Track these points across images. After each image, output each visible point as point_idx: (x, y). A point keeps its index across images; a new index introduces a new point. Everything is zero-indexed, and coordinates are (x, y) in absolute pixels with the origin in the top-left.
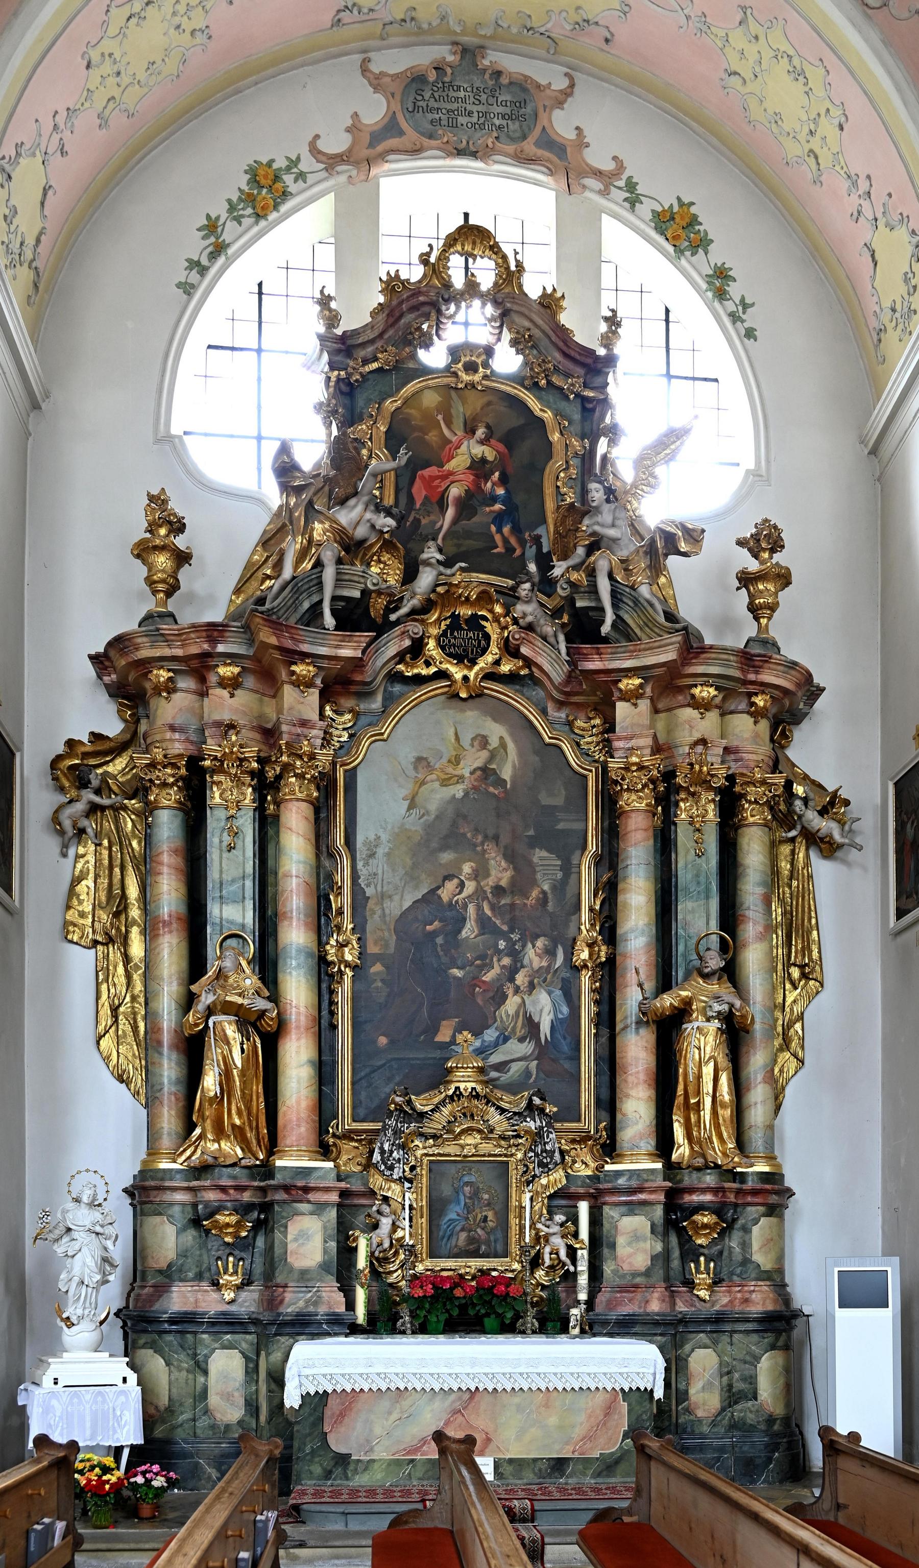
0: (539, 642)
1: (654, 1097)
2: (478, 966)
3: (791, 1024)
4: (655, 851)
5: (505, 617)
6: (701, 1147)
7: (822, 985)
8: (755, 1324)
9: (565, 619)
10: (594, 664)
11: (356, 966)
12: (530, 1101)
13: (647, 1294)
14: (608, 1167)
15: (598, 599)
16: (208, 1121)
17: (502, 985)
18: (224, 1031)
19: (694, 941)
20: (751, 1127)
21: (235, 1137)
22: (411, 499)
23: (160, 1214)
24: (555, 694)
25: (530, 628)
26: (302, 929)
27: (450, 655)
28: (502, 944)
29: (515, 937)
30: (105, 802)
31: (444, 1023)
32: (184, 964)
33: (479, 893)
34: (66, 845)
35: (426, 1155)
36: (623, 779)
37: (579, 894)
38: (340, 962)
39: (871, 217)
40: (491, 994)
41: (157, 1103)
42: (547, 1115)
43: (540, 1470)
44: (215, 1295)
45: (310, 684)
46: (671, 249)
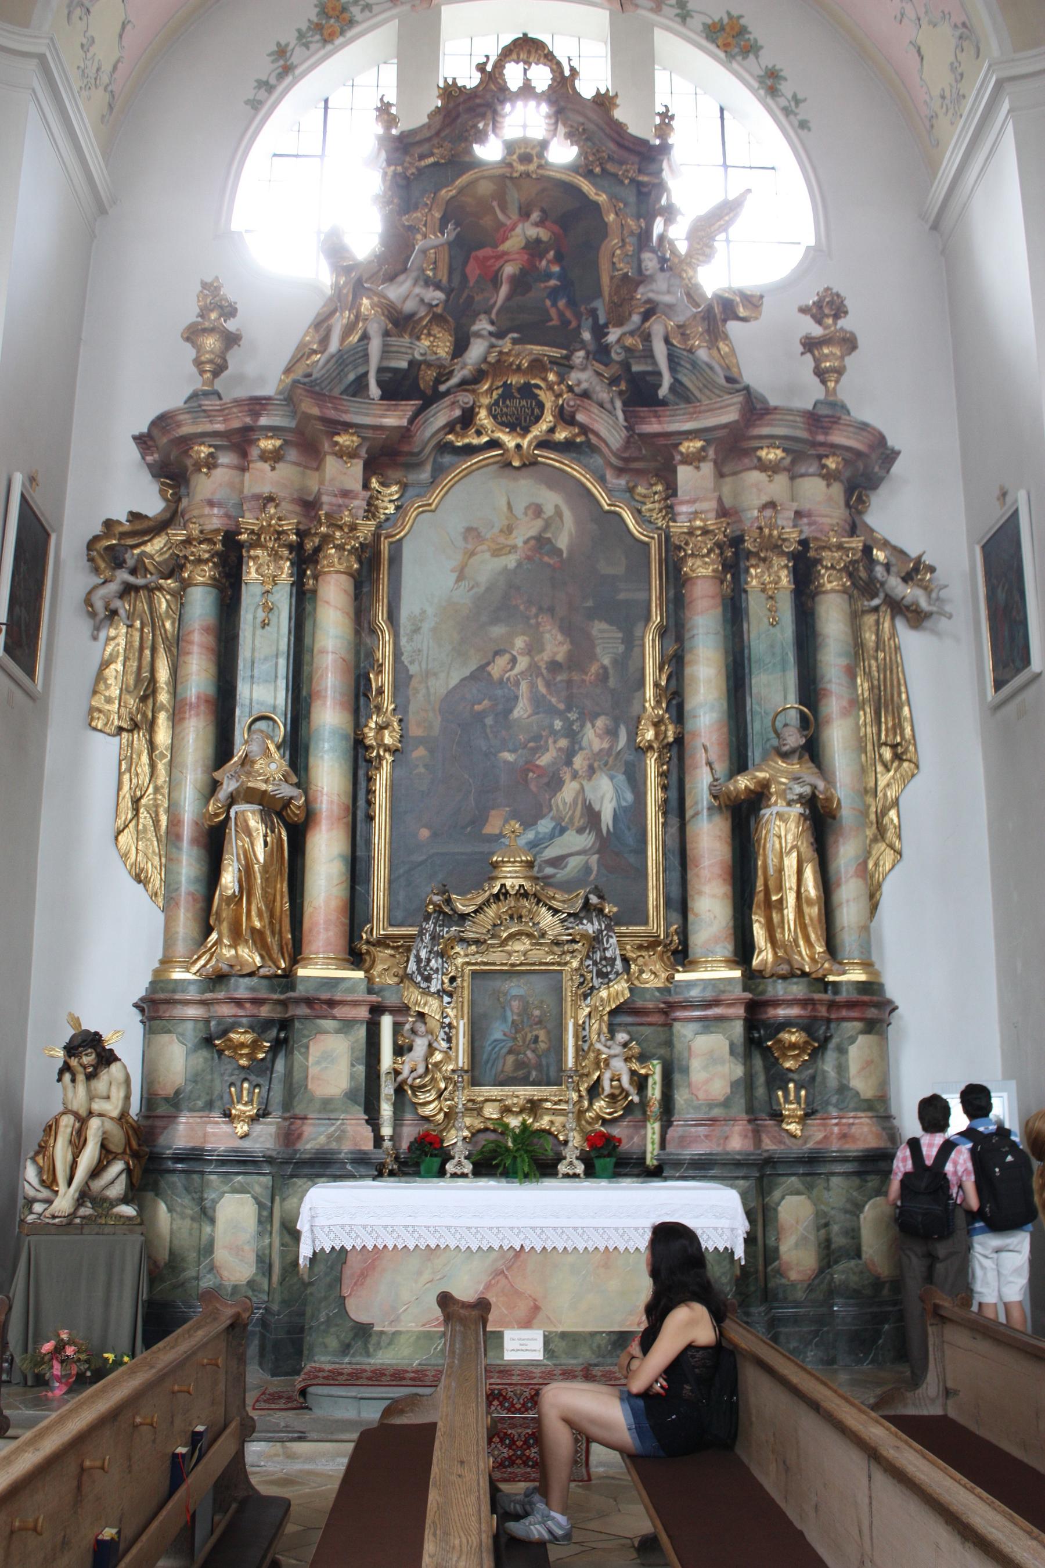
0: (595, 409)
2: (532, 749)
3: (884, 812)
4: (725, 621)
5: (559, 384)
7: (917, 767)
8: (856, 1164)
9: (623, 387)
10: (653, 427)
11: (397, 750)
12: (587, 900)
13: (726, 1128)
14: (679, 977)
15: (655, 363)
17: (559, 770)
19: (771, 717)
21: (254, 943)
22: (464, 278)
23: (169, 1032)
24: (614, 460)
25: (586, 395)
27: (503, 424)
28: (558, 724)
29: (573, 716)
30: (140, 581)
31: (493, 812)
32: (209, 751)
33: (533, 669)
34: (97, 628)
35: (468, 964)
36: (687, 544)
37: (643, 669)
38: (379, 746)
39: (914, 17)
40: (545, 780)
42: (606, 916)
43: (599, 1347)
44: (225, 1128)
45: (353, 455)
46: (722, 55)
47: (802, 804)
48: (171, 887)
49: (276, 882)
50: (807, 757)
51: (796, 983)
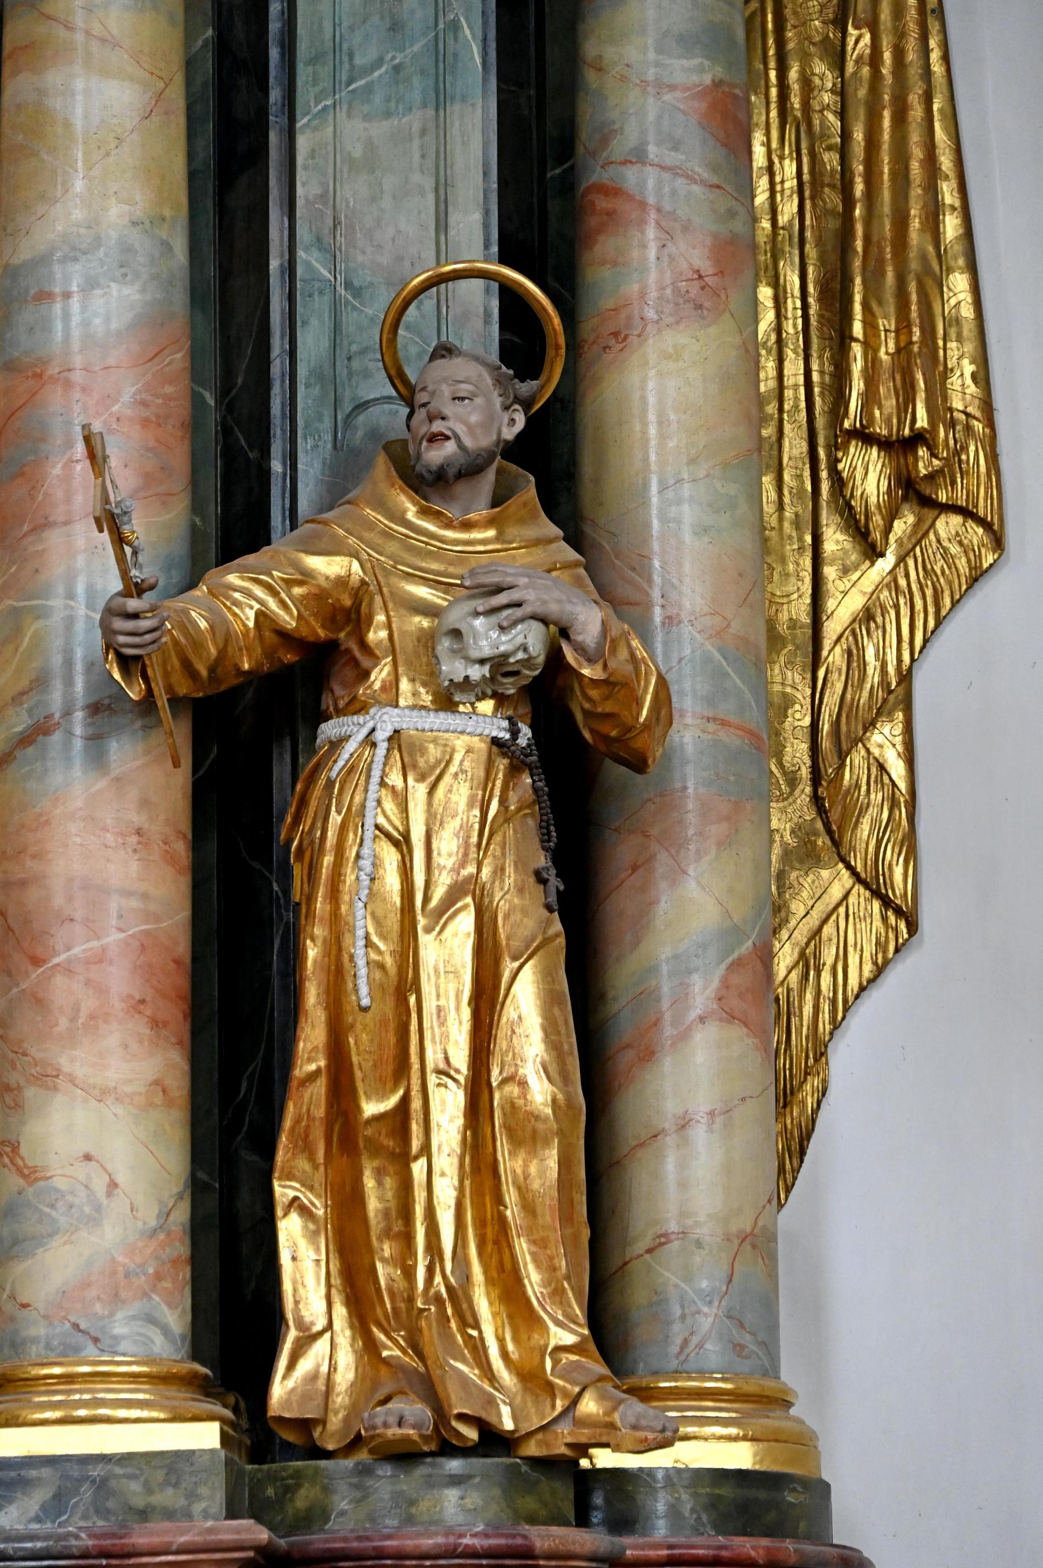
1: (179, 1083)
6: (415, 1346)
7: (998, 543)
19: (378, 306)
20: (662, 1240)
47: (501, 700)
50: (529, 491)
51: (456, 1481)
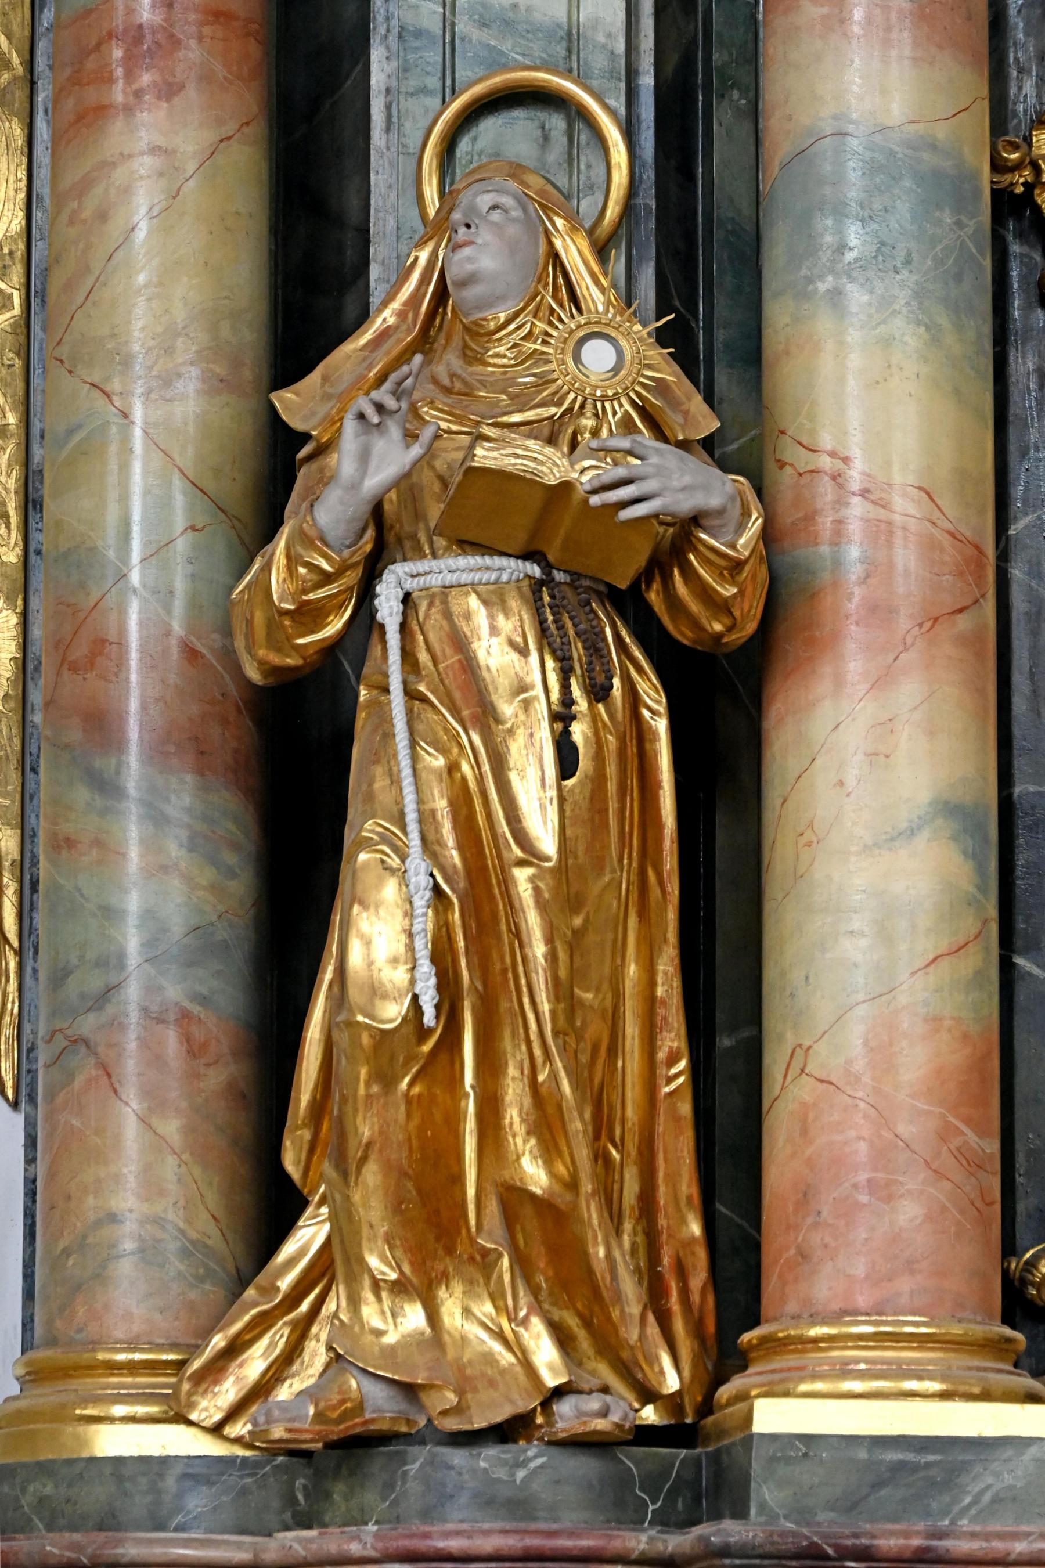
16: (372, 1175)
18: (460, 643)
21: (522, 1264)
26: (904, 38)
41: (86, 1071)
48: (72, 988)
49: (619, 949)
